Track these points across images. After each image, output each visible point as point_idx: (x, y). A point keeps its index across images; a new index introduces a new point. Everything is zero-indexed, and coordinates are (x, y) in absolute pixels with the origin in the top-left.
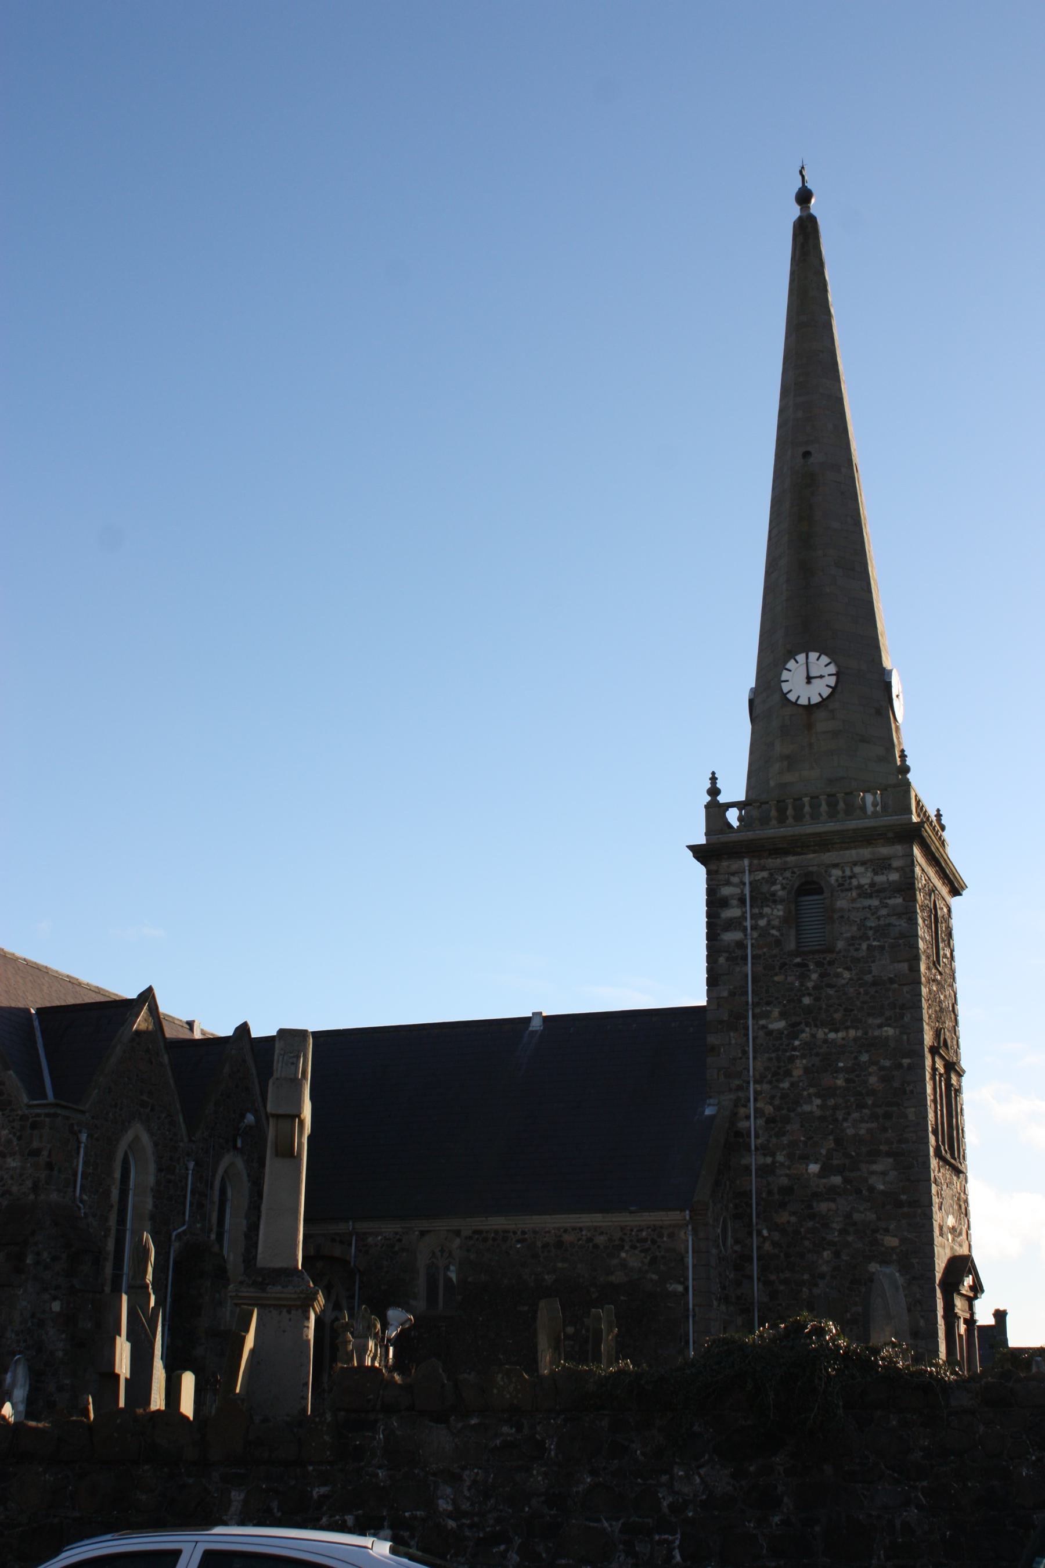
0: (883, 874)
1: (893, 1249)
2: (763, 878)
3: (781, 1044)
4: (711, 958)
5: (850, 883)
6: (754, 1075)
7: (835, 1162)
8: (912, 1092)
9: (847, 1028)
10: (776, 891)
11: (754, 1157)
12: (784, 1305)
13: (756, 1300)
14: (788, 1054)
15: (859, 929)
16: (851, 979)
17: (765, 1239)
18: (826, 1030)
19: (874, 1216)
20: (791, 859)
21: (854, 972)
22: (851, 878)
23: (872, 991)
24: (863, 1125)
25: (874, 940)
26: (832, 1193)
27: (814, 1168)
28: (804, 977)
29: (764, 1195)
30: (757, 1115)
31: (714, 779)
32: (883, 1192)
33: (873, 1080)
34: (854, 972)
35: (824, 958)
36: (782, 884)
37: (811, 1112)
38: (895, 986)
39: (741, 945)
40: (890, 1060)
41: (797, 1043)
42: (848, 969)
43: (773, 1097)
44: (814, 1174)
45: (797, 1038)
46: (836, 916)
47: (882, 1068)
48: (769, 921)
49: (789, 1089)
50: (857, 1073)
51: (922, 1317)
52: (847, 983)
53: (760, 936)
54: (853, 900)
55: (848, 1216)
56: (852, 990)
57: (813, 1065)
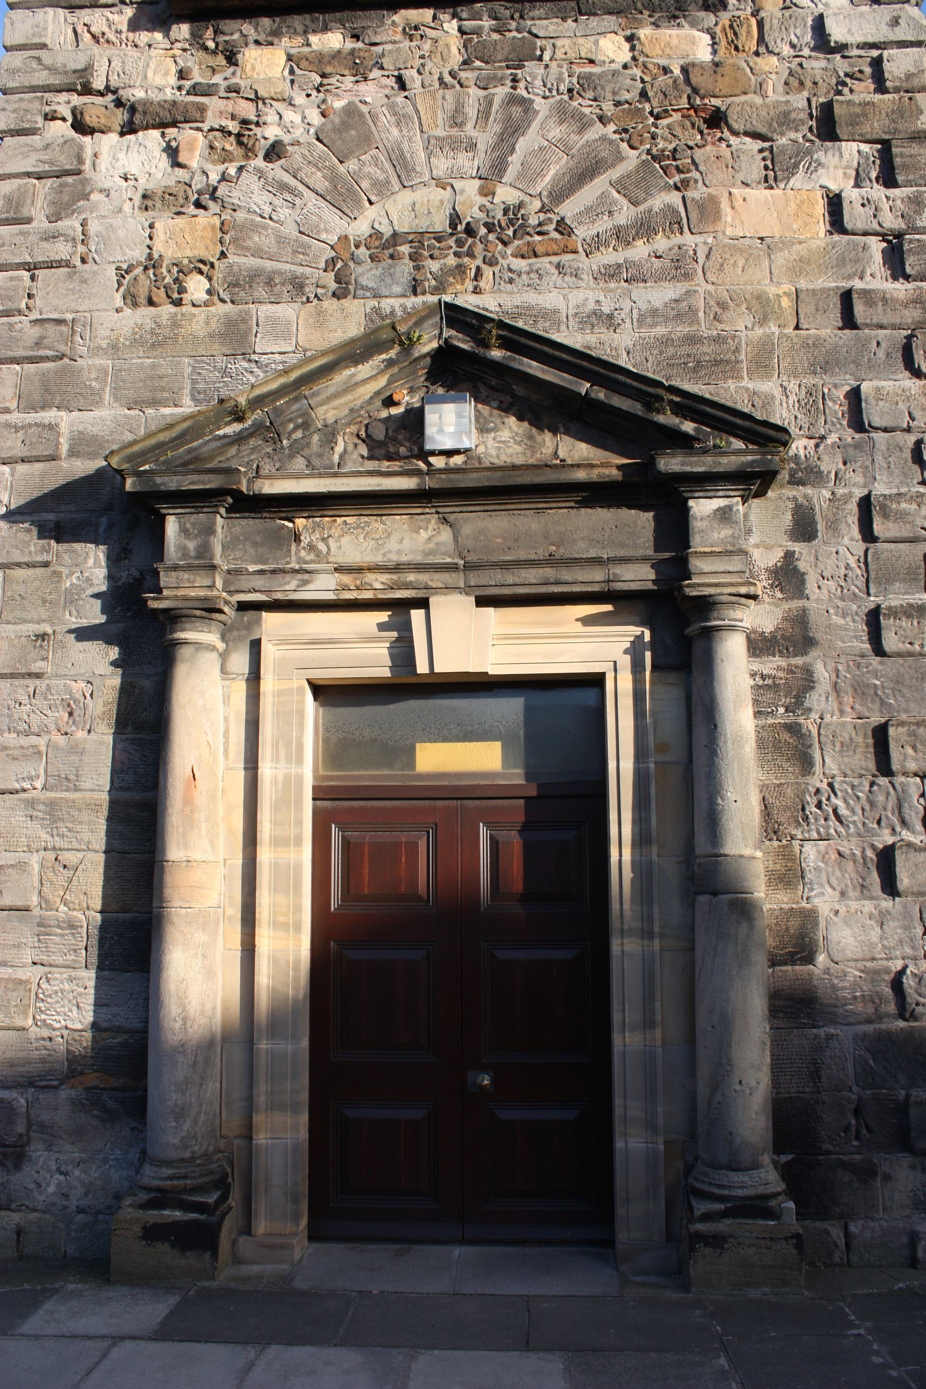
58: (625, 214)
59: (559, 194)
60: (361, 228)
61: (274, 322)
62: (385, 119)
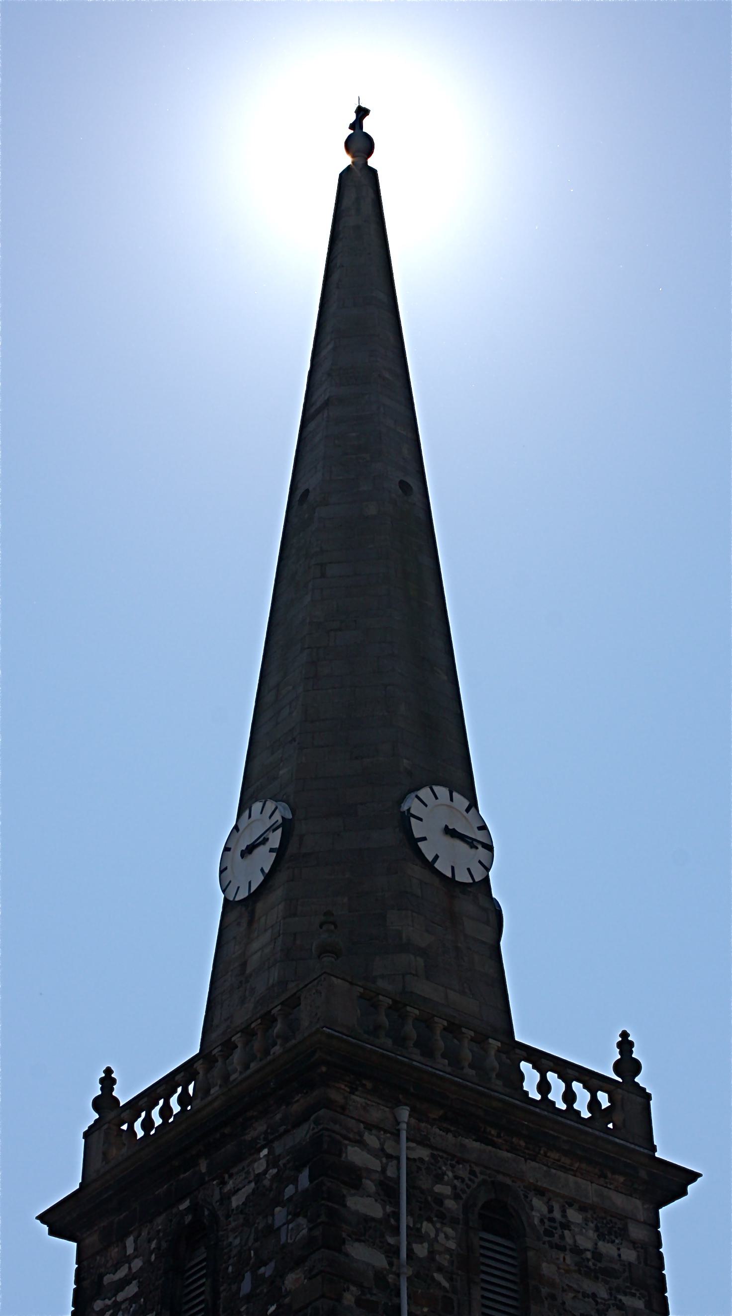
5: (562, 1237)
36: (454, 1187)
48: (432, 1253)
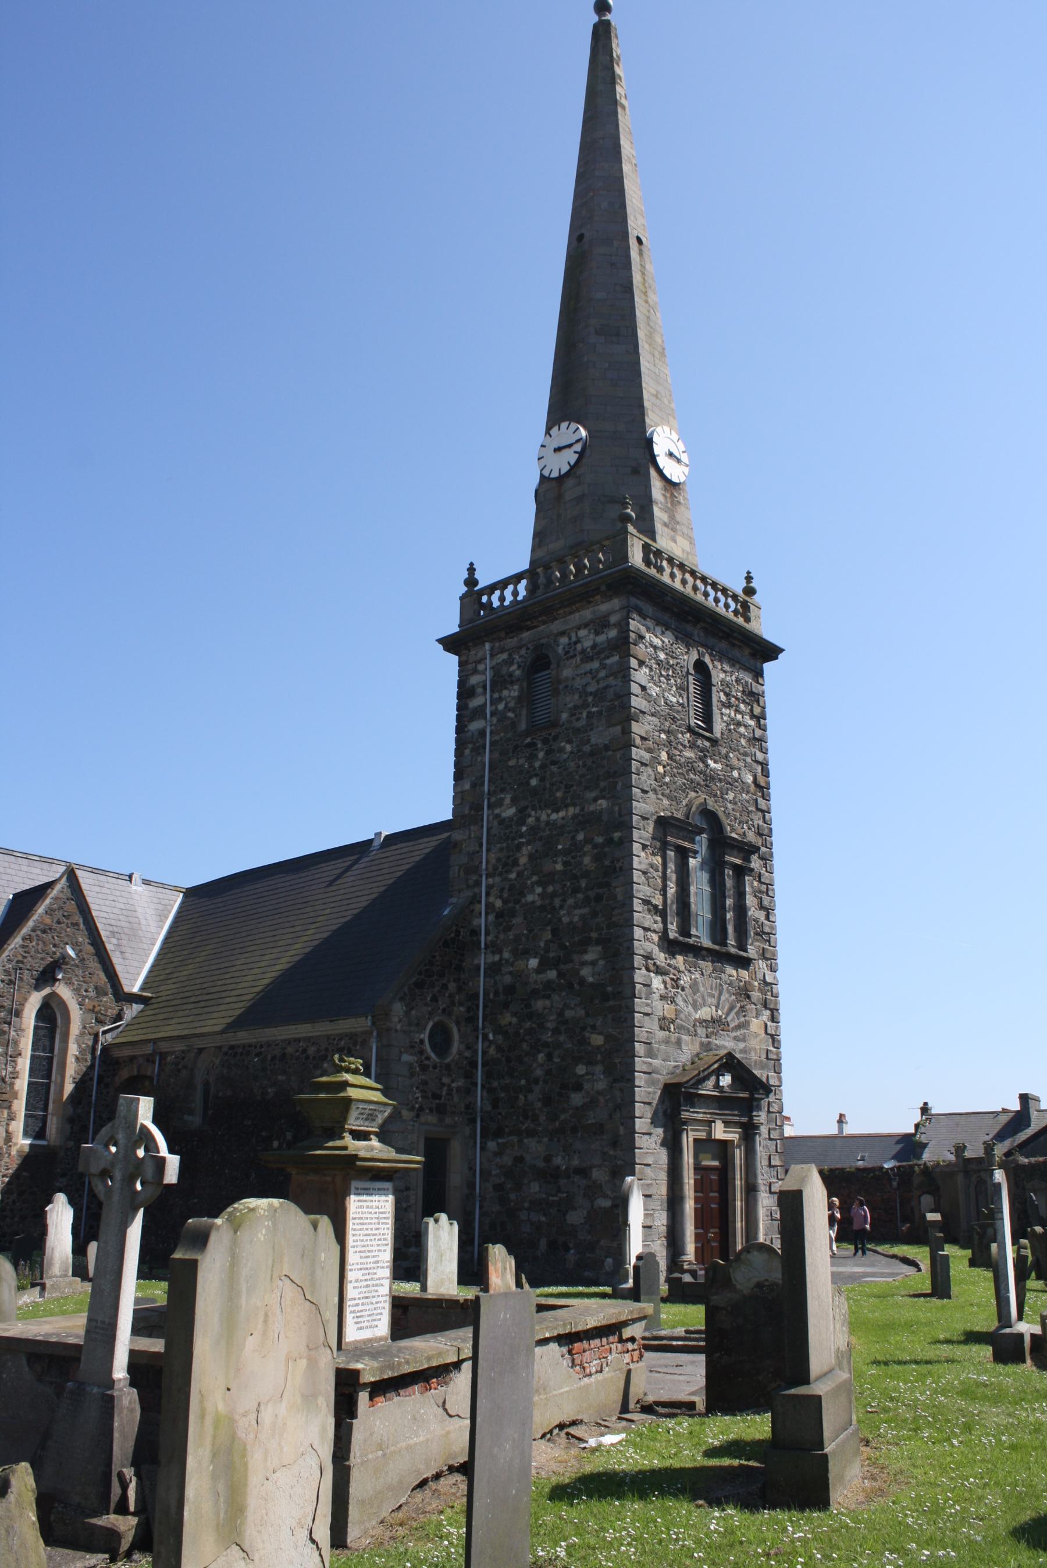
0: (603, 633)
1: (598, 1048)
2: (503, 660)
3: (511, 832)
4: (459, 752)
5: (575, 649)
6: (487, 869)
7: (552, 955)
8: (621, 868)
9: (567, 806)
10: (514, 671)
11: (483, 956)
12: (503, 1114)
13: (479, 1109)
14: (516, 842)
15: (580, 697)
16: (572, 752)
17: (491, 1042)
18: (549, 812)
19: (583, 1012)
20: (526, 635)
21: (575, 744)
22: (576, 643)
23: (589, 762)
24: (577, 912)
25: (593, 706)
26: (549, 987)
27: (533, 963)
28: (533, 757)
29: (491, 996)
30: (489, 911)
31: (471, 569)
32: (592, 984)
33: (587, 860)
34: (575, 744)
35: (550, 734)
37: (533, 902)
38: (610, 753)
39: (482, 733)
40: (603, 836)
41: (524, 829)
42: (569, 742)
43: (502, 890)
44: (533, 969)
45: (524, 823)
46: (561, 687)
47: (595, 846)
48: (506, 704)
49: (515, 879)
50: (573, 854)
51: (622, 1124)
52: (568, 758)
53: (498, 721)
54: (577, 667)
55: (561, 1014)
56: (572, 764)
57: (537, 851)
58: (737, 1022)
59: (728, 1014)
60: (697, 1016)
61: (686, 1041)
62: (701, 984)
